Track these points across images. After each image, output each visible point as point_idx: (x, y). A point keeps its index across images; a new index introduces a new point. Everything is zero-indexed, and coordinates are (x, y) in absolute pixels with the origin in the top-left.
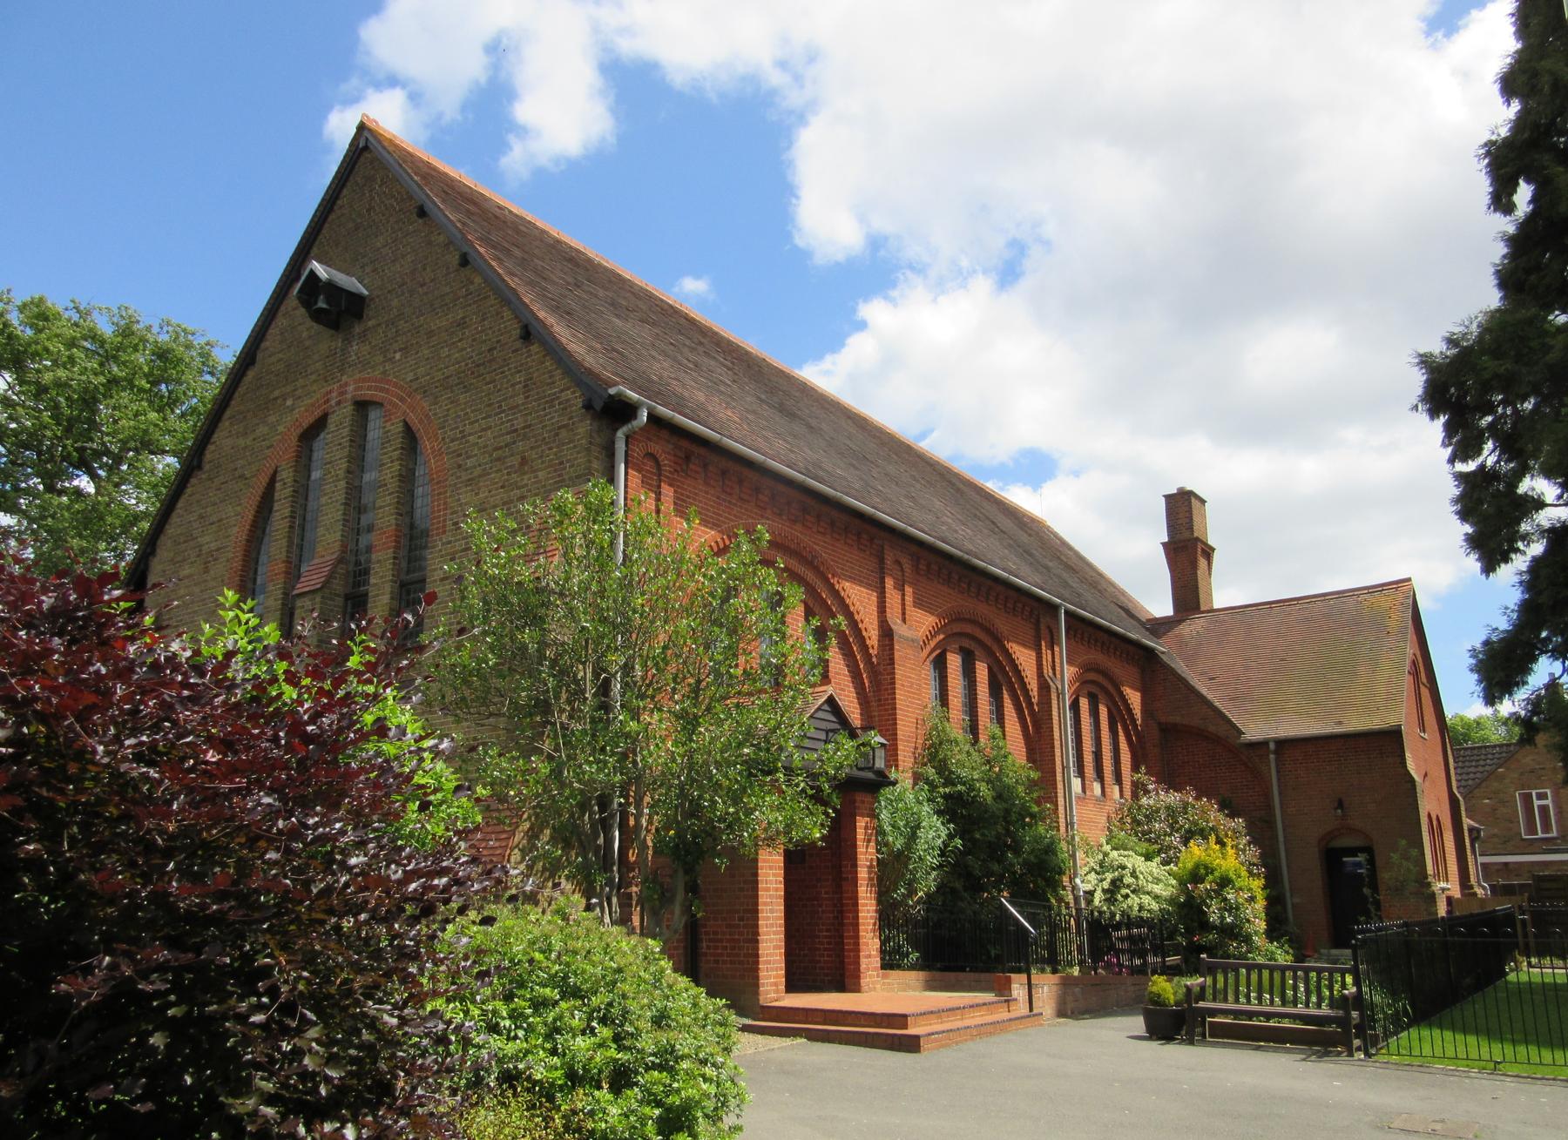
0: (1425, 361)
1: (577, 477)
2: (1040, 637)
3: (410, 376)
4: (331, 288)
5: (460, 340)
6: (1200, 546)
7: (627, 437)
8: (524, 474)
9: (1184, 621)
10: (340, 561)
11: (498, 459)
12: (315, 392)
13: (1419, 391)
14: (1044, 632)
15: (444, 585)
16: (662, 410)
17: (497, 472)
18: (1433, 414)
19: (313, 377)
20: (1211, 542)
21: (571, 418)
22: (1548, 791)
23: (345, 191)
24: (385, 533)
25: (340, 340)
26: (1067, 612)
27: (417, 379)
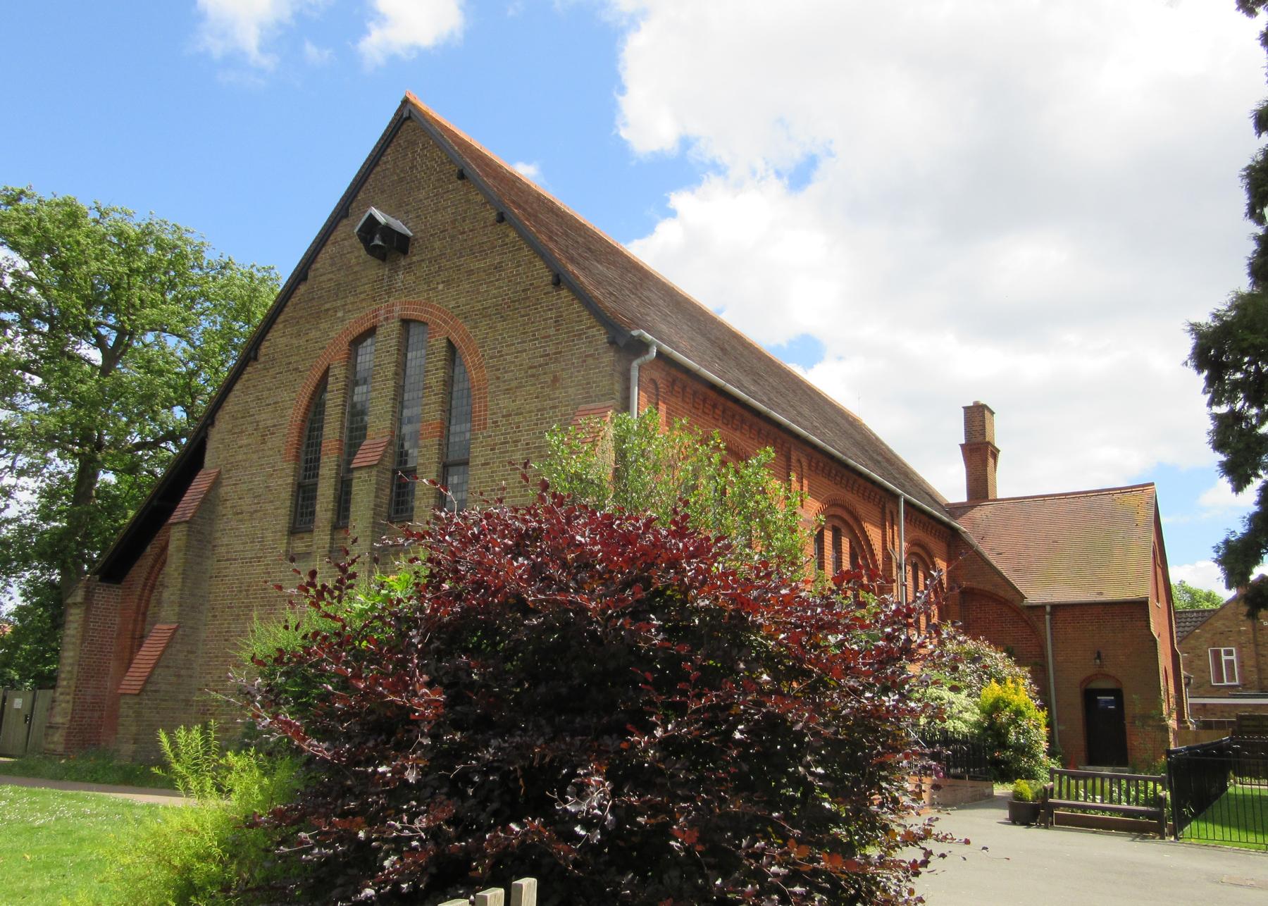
0: (1195, 329)
1: (602, 395)
2: (886, 519)
3: (452, 304)
4: (387, 231)
5: (497, 280)
6: (990, 448)
7: (640, 367)
8: (556, 389)
9: (975, 506)
10: (390, 443)
11: (533, 376)
12: (364, 308)
13: (1189, 351)
14: (888, 517)
15: (485, 469)
16: (666, 348)
17: (532, 385)
18: (1199, 368)
19: (363, 296)
20: (997, 445)
21: (597, 350)
23: (389, 150)
24: (430, 425)
25: (387, 269)
26: (907, 502)
27: (459, 306)
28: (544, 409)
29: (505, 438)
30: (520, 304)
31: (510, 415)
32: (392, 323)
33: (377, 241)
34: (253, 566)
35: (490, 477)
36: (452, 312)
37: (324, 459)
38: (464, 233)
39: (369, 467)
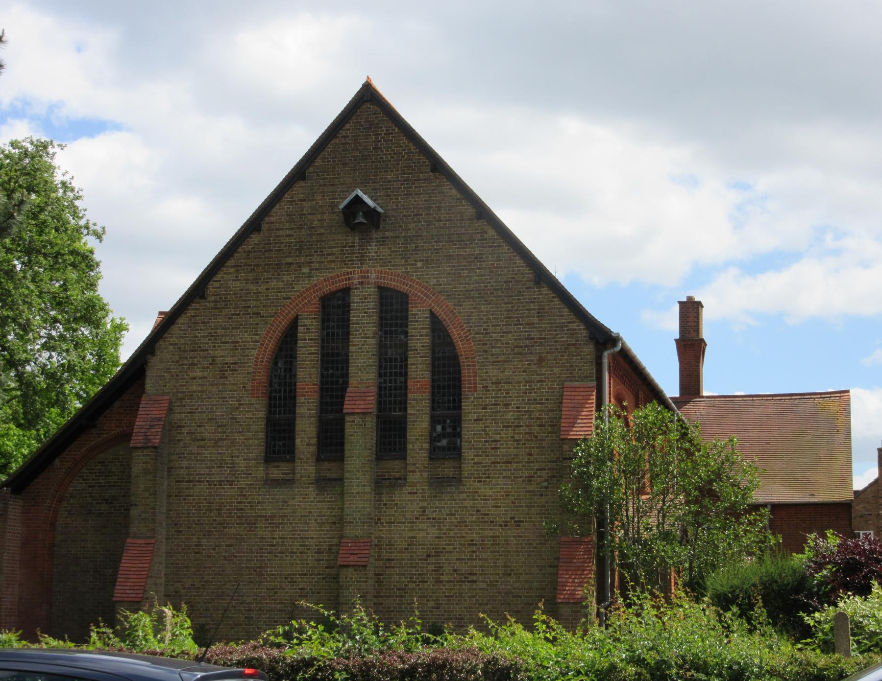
1: (584, 377)
3: (433, 282)
5: (479, 269)
8: (542, 367)
9: (688, 402)
12: (333, 269)
15: (478, 424)
17: (520, 361)
19: (330, 258)
21: (578, 341)
22: (872, 532)
23: (347, 126)
24: (419, 382)
25: (357, 238)
27: (441, 285)
28: (531, 382)
29: (495, 401)
30: (503, 292)
31: (500, 383)
32: (368, 288)
33: (360, 219)
34: (224, 488)
35: (483, 430)
36: (434, 289)
37: (300, 400)
38: (441, 221)
39: (363, 413)
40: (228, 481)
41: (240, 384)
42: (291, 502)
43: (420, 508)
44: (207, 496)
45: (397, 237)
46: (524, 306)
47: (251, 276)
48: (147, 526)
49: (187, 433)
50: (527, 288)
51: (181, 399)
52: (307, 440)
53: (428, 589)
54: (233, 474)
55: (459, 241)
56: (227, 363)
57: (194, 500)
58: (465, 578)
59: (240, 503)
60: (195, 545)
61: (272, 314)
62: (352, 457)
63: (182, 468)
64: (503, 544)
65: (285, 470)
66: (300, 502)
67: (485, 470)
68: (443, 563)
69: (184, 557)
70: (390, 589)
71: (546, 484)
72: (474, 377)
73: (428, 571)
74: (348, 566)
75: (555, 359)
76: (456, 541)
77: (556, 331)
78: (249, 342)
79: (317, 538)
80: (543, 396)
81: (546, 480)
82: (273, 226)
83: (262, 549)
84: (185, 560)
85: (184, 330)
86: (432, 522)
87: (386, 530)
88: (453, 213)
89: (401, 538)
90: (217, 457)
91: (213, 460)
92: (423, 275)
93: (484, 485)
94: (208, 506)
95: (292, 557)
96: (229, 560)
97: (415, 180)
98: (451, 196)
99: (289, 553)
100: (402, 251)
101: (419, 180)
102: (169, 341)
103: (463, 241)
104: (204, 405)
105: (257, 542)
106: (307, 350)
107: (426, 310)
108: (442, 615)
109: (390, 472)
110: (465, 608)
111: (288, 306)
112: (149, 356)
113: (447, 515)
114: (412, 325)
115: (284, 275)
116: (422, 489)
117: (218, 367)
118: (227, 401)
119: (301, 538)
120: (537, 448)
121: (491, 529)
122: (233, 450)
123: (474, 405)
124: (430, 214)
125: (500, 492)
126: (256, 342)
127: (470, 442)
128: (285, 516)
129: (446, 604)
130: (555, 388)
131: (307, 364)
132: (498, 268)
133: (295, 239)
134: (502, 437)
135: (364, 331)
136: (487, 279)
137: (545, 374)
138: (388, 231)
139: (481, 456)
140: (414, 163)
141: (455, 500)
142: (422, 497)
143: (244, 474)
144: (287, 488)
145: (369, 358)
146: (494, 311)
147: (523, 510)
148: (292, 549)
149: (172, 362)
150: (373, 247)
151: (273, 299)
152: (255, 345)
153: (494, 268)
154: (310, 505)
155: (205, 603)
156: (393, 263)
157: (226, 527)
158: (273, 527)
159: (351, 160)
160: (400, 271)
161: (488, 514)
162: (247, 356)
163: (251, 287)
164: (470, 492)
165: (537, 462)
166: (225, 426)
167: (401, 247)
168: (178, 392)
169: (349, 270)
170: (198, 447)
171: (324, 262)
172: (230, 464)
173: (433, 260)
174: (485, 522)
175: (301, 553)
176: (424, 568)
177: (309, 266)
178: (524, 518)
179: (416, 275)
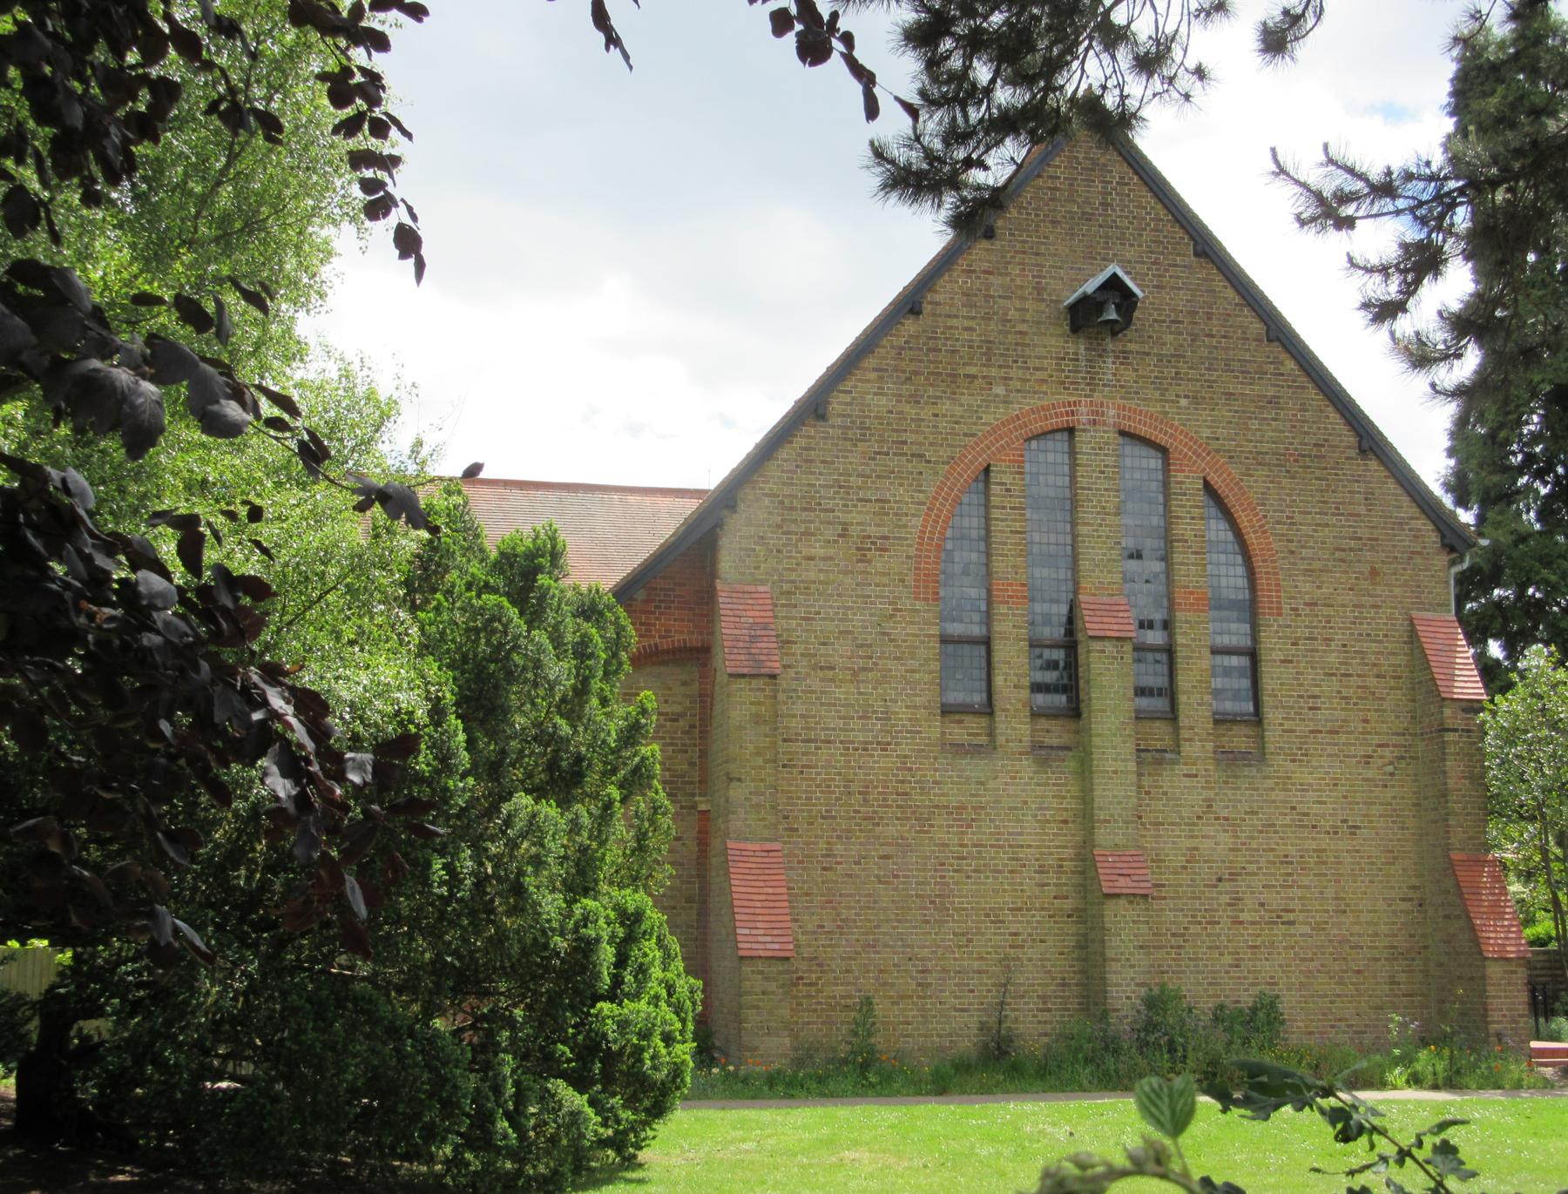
1: (1438, 605)
3: (1206, 433)
12: (1046, 393)
19: (1040, 375)
21: (1425, 548)
24: (1192, 593)
25: (1082, 347)
27: (1218, 439)
28: (1361, 606)
29: (1311, 633)
30: (1312, 461)
32: (1104, 432)
34: (873, 756)
35: (1295, 679)
36: (1208, 444)
38: (1213, 336)
39: (1118, 639)
40: (878, 743)
41: (895, 574)
42: (991, 784)
43: (1204, 800)
44: (842, 768)
45: (1148, 354)
46: (1344, 486)
47: (907, 389)
48: (763, 819)
49: (802, 655)
50: (1347, 458)
51: (789, 593)
52: (1015, 679)
53: (1220, 935)
54: (888, 732)
55: (1243, 372)
56: (869, 537)
57: (818, 774)
58: (1279, 917)
59: (903, 782)
60: (823, 856)
61: (945, 459)
62: (1104, 711)
63: (794, 716)
64: (1332, 863)
65: (972, 728)
66: (1006, 784)
67: (1301, 743)
68: (1243, 893)
69: (802, 876)
70: (1161, 935)
71: (1390, 768)
72: (1277, 591)
73: (1220, 905)
74: (1117, 896)
75: (1395, 574)
76: (1261, 856)
77: (1393, 529)
78: (907, 503)
79: (1038, 847)
80: (1380, 630)
81: (1391, 763)
82: (939, 310)
83: (943, 864)
84: (804, 882)
85: (790, 471)
86: (1223, 825)
87: (1151, 836)
88: (1231, 326)
89: (1176, 849)
90: (857, 700)
91: (852, 706)
92: (1189, 420)
93: (1300, 766)
94: (845, 787)
95: (997, 878)
96: (888, 883)
97: (1170, 265)
98: (1226, 298)
99: (991, 871)
100: (1156, 377)
101: (1175, 265)
102: (763, 489)
103: (1250, 373)
104: (831, 607)
105: (934, 852)
106: (1008, 526)
107: (1198, 478)
108: (1245, 978)
109: (1147, 740)
110: (1280, 966)
111: (973, 449)
112: (725, 512)
113: (1246, 813)
114: (1177, 500)
115: (963, 394)
116: (1206, 770)
117: (853, 543)
118: (872, 603)
119: (1010, 846)
120: (1376, 711)
121: (1314, 839)
122: (885, 689)
123: (1279, 638)
124: (1196, 323)
125: (1324, 779)
126: (920, 503)
127: (1276, 696)
128: (982, 808)
129: (1249, 960)
130: (1397, 619)
131: (1010, 550)
132: (1303, 422)
133: (980, 335)
134: (1323, 692)
135: (1100, 501)
136: (1287, 437)
137: (1381, 596)
138: (1130, 341)
139: (1294, 719)
140: (1165, 237)
141: (1257, 789)
142: (1207, 782)
143: (907, 732)
144: (982, 759)
145: (1111, 548)
146: (1301, 490)
147: (1359, 809)
148: (995, 865)
149: (769, 526)
150: (1110, 364)
151: (947, 434)
152: (919, 510)
153: (1298, 421)
154: (1023, 791)
155: (842, 959)
156: (1141, 396)
157: (878, 824)
158: (962, 826)
159: (1065, 217)
160: (1155, 409)
161: (1308, 814)
162: (905, 526)
163: (907, 408)
164: (1278, 778)
165: (1376, 733)
166: (870, 646)
167: (1153, 371)
168: (782, 581)
169: (1072, 399)
170: (822, 680)
171: (1029, 380)
172: (882, 713)
173: (1204, 398)
174: (1304, 826)
175: (1012, 872)
176: (1212, 899)
177: (1005, 385)
178: (1361, 821)
179: (1180, 419)
